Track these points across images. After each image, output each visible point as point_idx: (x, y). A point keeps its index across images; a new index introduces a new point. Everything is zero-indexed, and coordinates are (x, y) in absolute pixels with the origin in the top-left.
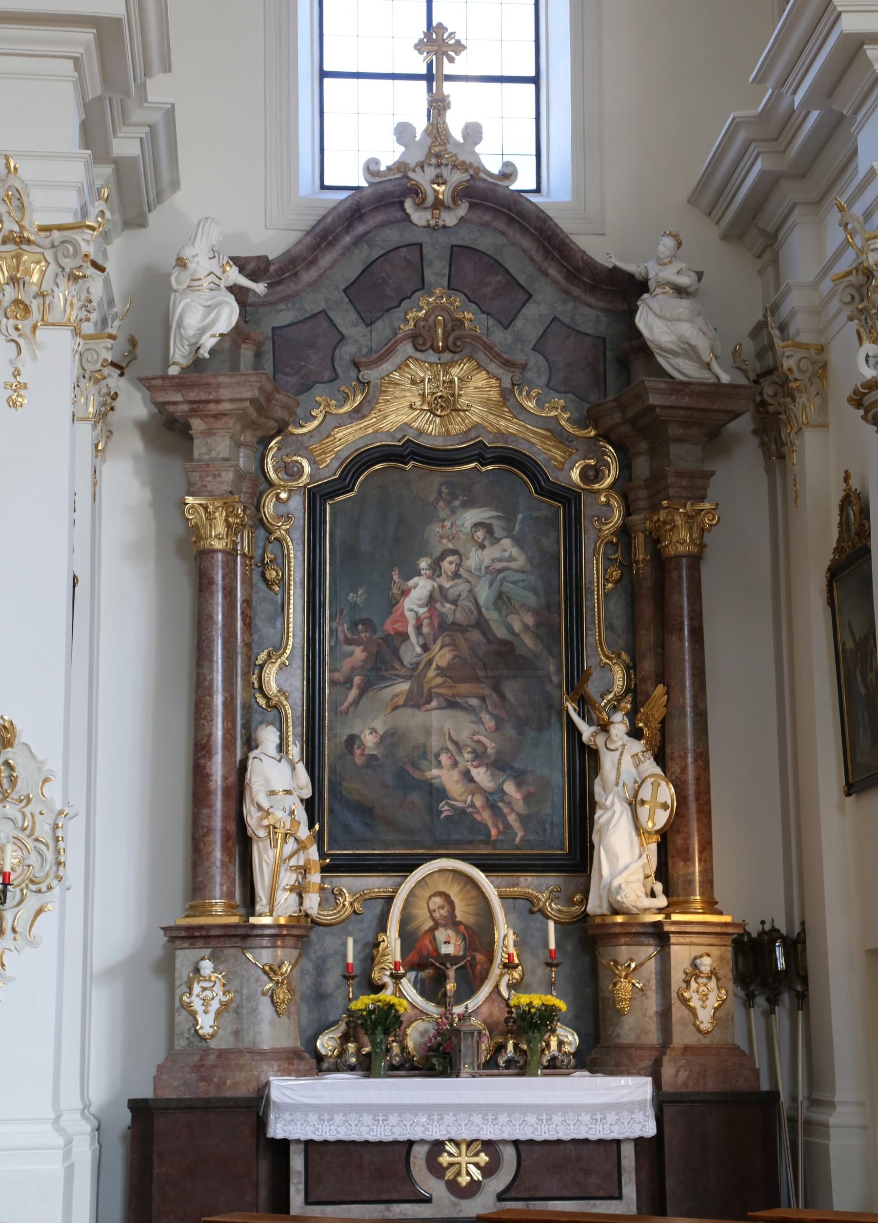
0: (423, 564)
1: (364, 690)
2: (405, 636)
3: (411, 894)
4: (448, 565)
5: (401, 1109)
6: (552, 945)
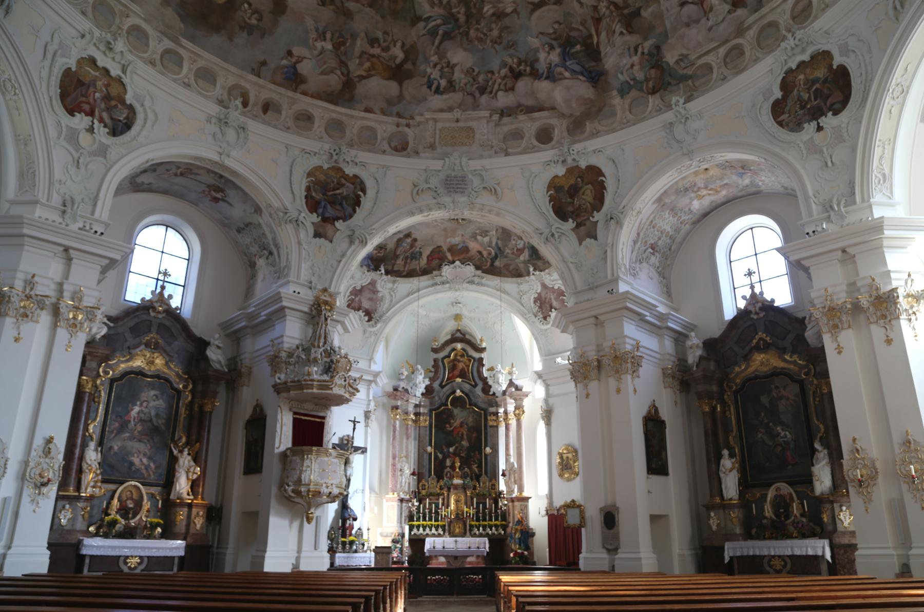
0: (138, 403)
1: (116, 434)
2: (130, 421)
3: (122, 491)
4: (145, 404)
5: (119, 547)
6: (160, 506)
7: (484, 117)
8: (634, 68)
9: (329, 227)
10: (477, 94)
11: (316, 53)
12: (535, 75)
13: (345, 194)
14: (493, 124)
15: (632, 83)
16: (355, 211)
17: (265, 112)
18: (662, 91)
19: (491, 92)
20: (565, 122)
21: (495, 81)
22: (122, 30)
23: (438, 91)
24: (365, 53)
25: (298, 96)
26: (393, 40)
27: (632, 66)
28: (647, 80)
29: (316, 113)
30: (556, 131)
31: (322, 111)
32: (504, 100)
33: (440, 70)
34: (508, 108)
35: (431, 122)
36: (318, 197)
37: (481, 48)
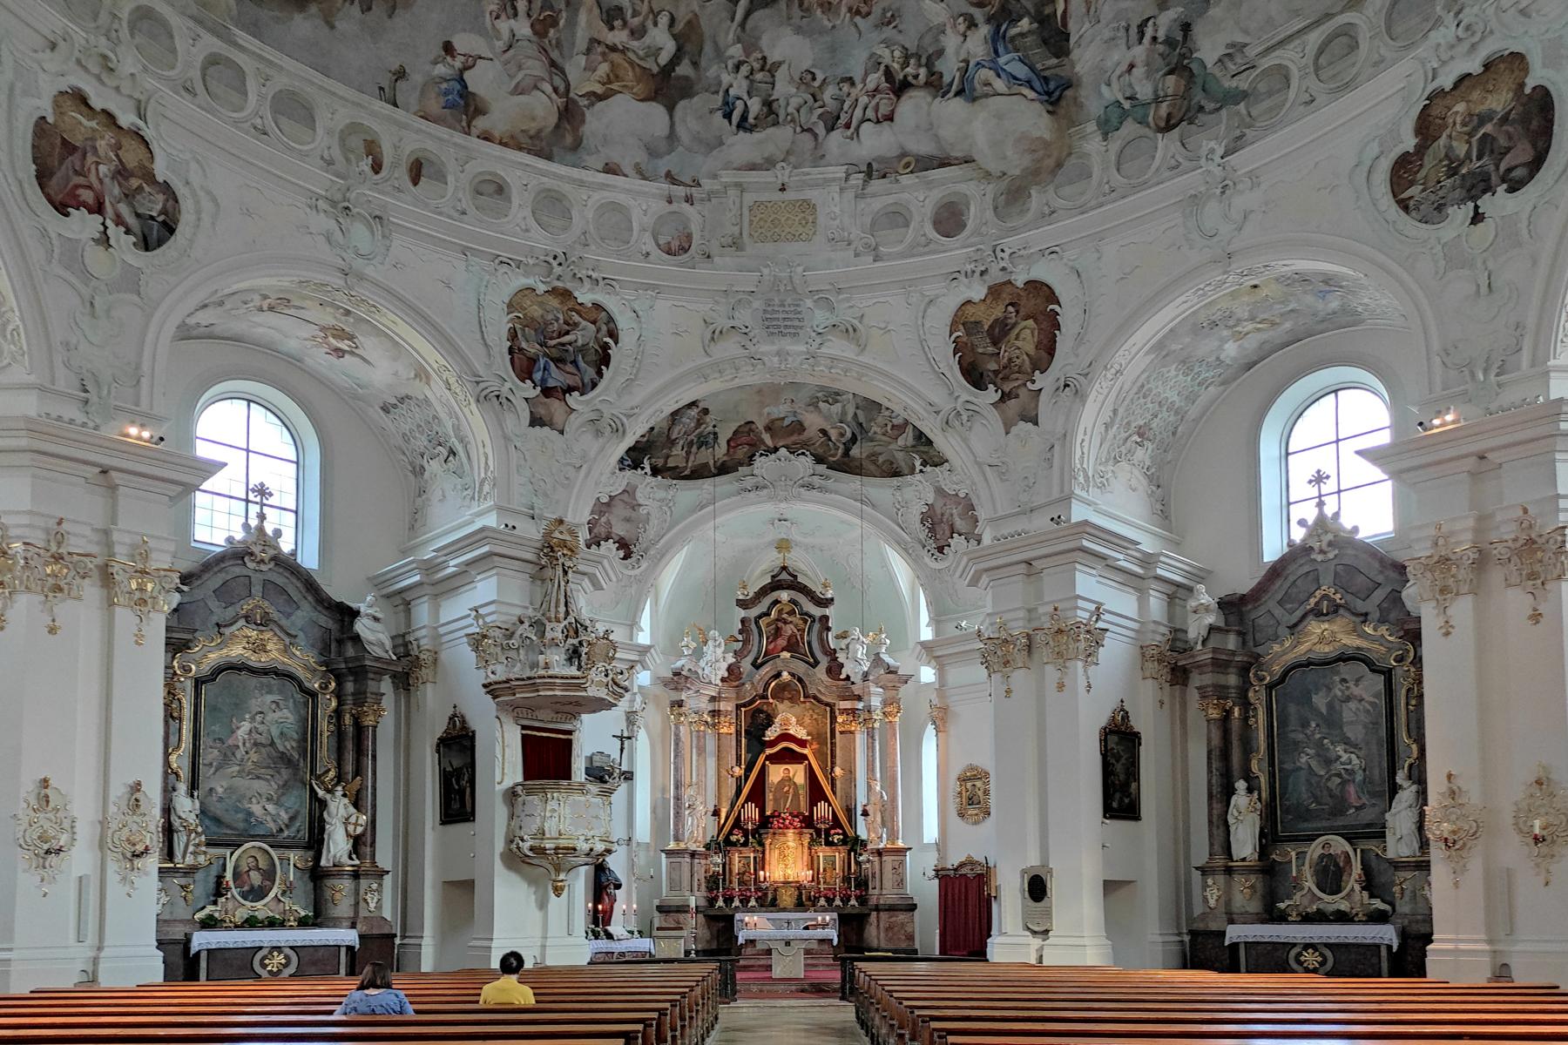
4: (258, 718)
7: (834, 180)
8: (1134, 70)
9: (555, 405)
10: (820, 129)
11: (500, 45)
12: (935, 85)
13: (580, 343)
14: (850, 194)
15: (1127, 105)
16: (600, 374)
17: (415, 182)
18: (1184, 123)
19: (848, 126)
20: (990, 189)
21: (857, 100)
22: (120, 19)
23: (743, 125)
24: (599, 43)
25: (474, 142)
26: (651, 10)
27: (1132, 66)
28: (1157, 100)
29: (513, 178)
30: (972, 209)
31: (520, 169)
32: (874, 142)
33: (747, 77)
34: (881, 160)
35: (732, 192)
36: (533, 351)
37: (830, 25)
